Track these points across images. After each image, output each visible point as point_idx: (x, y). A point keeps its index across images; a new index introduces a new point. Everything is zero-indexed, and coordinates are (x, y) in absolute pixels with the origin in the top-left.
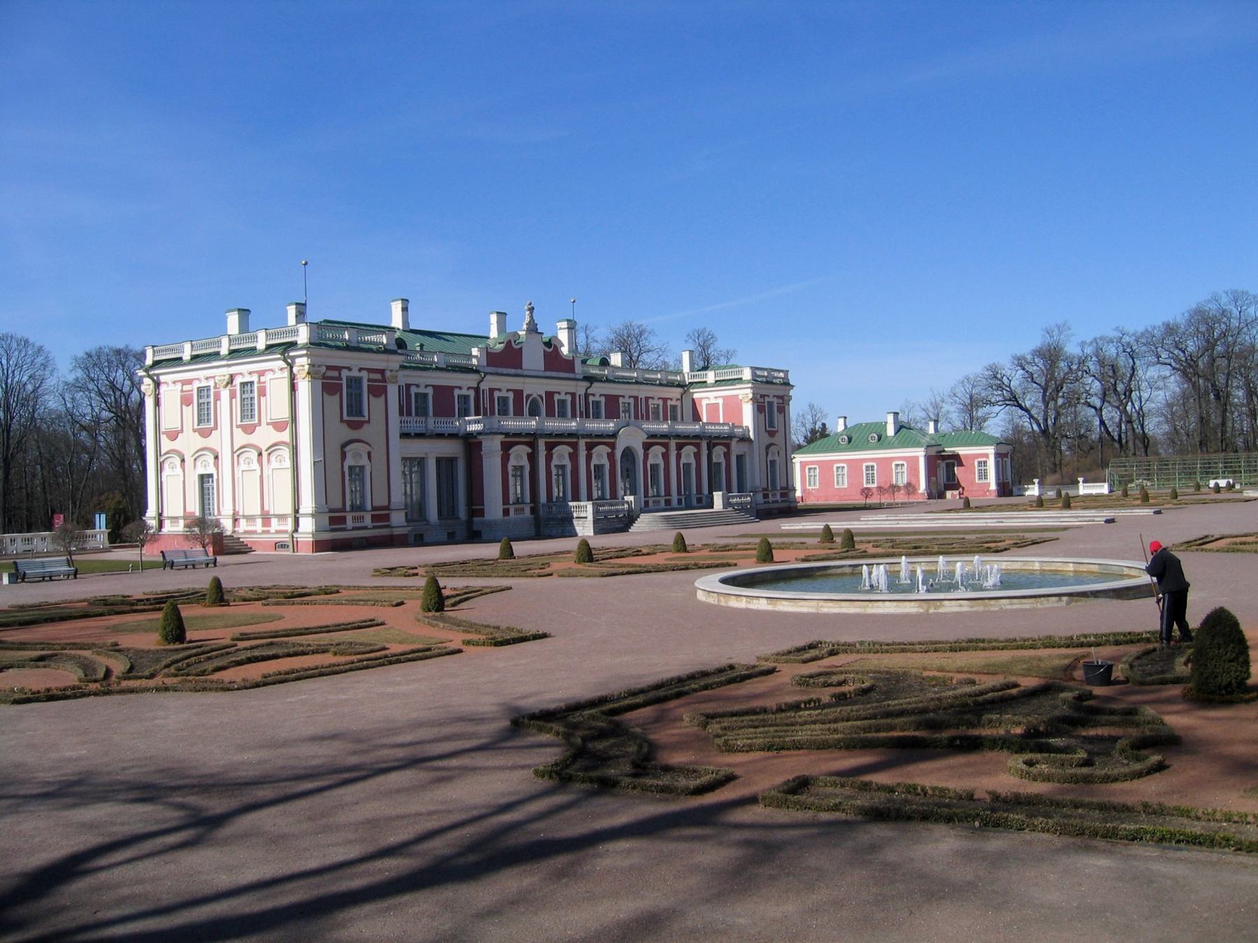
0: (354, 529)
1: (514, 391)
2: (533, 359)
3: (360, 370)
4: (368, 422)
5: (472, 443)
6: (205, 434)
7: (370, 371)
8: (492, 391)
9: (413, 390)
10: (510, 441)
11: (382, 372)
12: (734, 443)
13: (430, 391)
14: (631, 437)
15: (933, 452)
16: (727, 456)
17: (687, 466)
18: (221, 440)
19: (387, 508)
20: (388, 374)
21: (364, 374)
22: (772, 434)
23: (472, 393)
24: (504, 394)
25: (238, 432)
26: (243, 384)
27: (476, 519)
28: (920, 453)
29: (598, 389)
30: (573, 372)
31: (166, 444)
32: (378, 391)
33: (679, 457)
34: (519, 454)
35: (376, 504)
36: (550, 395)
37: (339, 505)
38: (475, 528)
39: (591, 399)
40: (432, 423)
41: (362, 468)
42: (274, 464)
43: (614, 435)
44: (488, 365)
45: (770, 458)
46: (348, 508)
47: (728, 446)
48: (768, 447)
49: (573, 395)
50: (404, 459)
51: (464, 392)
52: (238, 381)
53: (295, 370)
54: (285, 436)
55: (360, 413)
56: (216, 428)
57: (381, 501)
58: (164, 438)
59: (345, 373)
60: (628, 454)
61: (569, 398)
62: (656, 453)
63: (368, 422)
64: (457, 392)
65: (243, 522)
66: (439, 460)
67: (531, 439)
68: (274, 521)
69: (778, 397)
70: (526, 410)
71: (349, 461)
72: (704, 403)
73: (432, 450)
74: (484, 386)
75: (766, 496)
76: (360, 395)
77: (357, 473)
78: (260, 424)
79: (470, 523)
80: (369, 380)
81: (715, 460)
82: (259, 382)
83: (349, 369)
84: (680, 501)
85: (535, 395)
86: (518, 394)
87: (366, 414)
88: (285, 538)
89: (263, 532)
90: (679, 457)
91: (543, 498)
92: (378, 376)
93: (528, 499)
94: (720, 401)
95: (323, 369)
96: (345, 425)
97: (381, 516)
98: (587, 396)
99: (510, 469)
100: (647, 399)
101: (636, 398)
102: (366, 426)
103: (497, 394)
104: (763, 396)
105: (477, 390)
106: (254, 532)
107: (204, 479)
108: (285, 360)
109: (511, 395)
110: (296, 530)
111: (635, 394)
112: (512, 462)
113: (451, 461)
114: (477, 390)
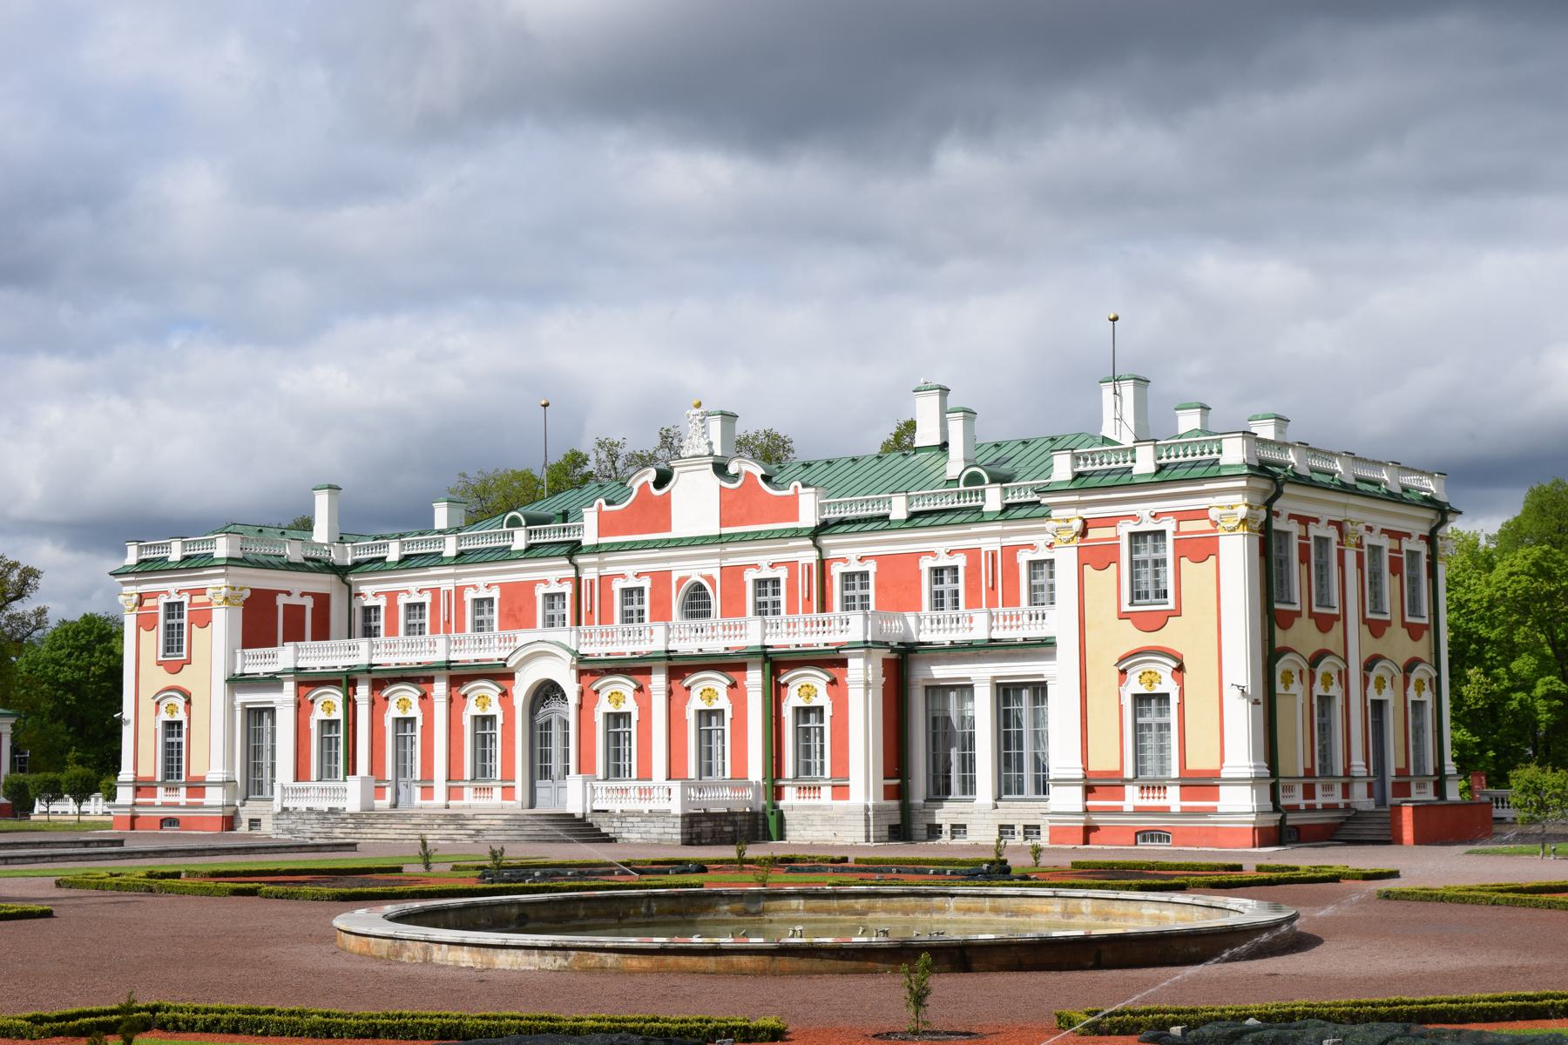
0: (164, 805)
1: (654, 575)
8: (605, 581)
9: (469, 595)
13: (495, 593)
14: (548, 655)
19: (202, 780)
23: (568, 589)
29: (848, 553)
36: (732, 575)
39: (836, 571)
41: (180, 724)
46: (159, 779)
48: (1122, 660)
49: (792, 565)
55: (180, 649)
60: (547, 691)
61: (782, 574)
62: (618, 694)
69: (1181, 516)
74: (589, 574)
77: (172, 727)
86: (662, 579)
97: (197, 787)
98: (823, 564)
99: (314, 726)
100: (1010, 552)
101: (973, 554)
105: (578, 581)
109: (646, 583)
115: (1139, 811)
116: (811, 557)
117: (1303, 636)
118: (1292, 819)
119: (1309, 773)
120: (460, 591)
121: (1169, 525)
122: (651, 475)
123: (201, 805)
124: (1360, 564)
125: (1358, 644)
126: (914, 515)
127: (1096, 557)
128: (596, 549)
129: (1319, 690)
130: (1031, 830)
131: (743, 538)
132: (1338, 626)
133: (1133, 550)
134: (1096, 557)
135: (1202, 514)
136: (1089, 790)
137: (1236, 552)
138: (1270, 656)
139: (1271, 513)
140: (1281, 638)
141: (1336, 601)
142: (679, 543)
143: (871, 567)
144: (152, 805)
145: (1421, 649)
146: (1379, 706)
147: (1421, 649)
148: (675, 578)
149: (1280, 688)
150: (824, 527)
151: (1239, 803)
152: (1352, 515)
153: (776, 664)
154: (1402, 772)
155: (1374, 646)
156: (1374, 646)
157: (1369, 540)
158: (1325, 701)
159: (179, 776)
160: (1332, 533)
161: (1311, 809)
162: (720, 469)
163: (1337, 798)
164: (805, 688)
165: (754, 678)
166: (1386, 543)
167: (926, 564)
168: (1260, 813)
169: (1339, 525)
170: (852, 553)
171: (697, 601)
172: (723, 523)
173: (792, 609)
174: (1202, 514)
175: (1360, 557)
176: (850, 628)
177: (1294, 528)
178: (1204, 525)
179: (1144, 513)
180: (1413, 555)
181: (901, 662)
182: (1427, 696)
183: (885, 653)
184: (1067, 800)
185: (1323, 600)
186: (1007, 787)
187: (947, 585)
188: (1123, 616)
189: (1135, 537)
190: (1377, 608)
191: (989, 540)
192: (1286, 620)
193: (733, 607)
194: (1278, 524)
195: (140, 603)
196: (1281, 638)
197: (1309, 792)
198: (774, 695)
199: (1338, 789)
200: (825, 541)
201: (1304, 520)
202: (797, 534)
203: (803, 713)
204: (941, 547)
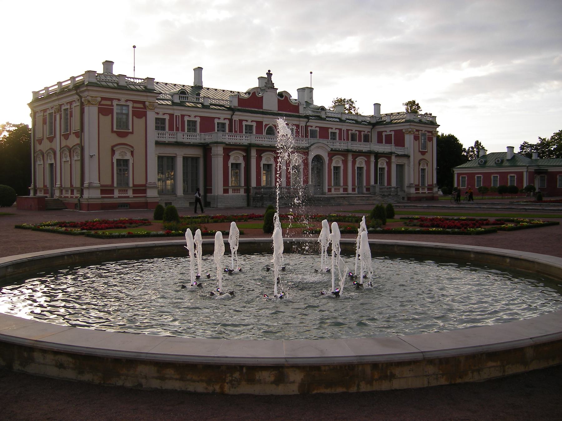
0: (119, 197)
1: (257, 122)
2: (270, 104)
3: (127, 101)
4: (132, 133)
5: (206, 148)
6: (51, 140)
7: (134, 102)
8: (241, 121)
9: (186, 119)
10: (228, 149)
11: (143, 103)
12: (393, 159)
13: (198, 120)
15: (532, 169)
16: (389, 164)
17: (360, 169)
18: (56, 145)
19: (145, 186)
20: (147, 104)
21: (130, 104)
22: (423, 153)
23: (227, 122)
24: (249, 123)
25: (62, 138)
26: (65, 110)
27: (208, 194)
28: (524, 170)
30: (298, 112)
31: (39, 147)
32: (140, 114)
33: (354, 163)
34: (237, 158)
35: (135, 183)
37: (109, 183)
38: (208, 200)
39: (309, 128)
40: (181, 137)
41: (127, 161)
42: (76, 158)
43: (308, 148)
44: (239, 106)
45: (421, 167)
47: (390, 158)
50: (160, 158)
51: (221, 121)
52: (63, 108)
53: (83, 99)
54: (77, 141)
56: (55, 137)
57: (140, 181)
58: (37, 143)
59: (115, 103)
60: (318, 158)
62: (337, 161)
63: (132, 133)
64: (216, 121)
65: (64, 191)
66: (185, 159)
67: (247, 149)
68: (75, 191)
69: (429, 132)
70: (264, 133)
71: (117, 156)
72: (384, 134)
73: (180, 154)
75: (417, 189)
76: (127, 115)
77: (123, 164)
78: (70, 134)
79: (205, 196)
80: (133, 107)
81: (379, 166)
82: (71, 108)
83: (119, 100)
84: (354, 190)
85: (271, 125)
86: (259, 124)
87: (130, 127)
88: (76, 201)
89: (72, 197)
90: (354, 163)
91: (254, 184)
92: (141, 106)
93: (243, 184)
94: (393, 133)
95: (99, 99)
96: (114, 135)
97: (140, 190)
98: (306, 127)
101: (340, 130)
102: (130, 136)
103: (244, 123)
104: (417, 131)
105: (231, 120)
106: (68, 197)
107: (51, 165)
108: (77, 94)
109: (254, 124)
110: (82, 197)
111: (340, 127)
112: (232, 161)
113: (195, 160)
114: (231, 120)
115: (422, 193)
120: (183, 116)
123: (145, 197)
127: (416, 138)
130: (403, 198)
144: (112, 197)
148: (264, 124)
153: (378, 156)
159: (127, 184)
164: (382, 163)
165: (373, 159)
172: (279, 109)
178: (430, 134)
195: (100, 102)
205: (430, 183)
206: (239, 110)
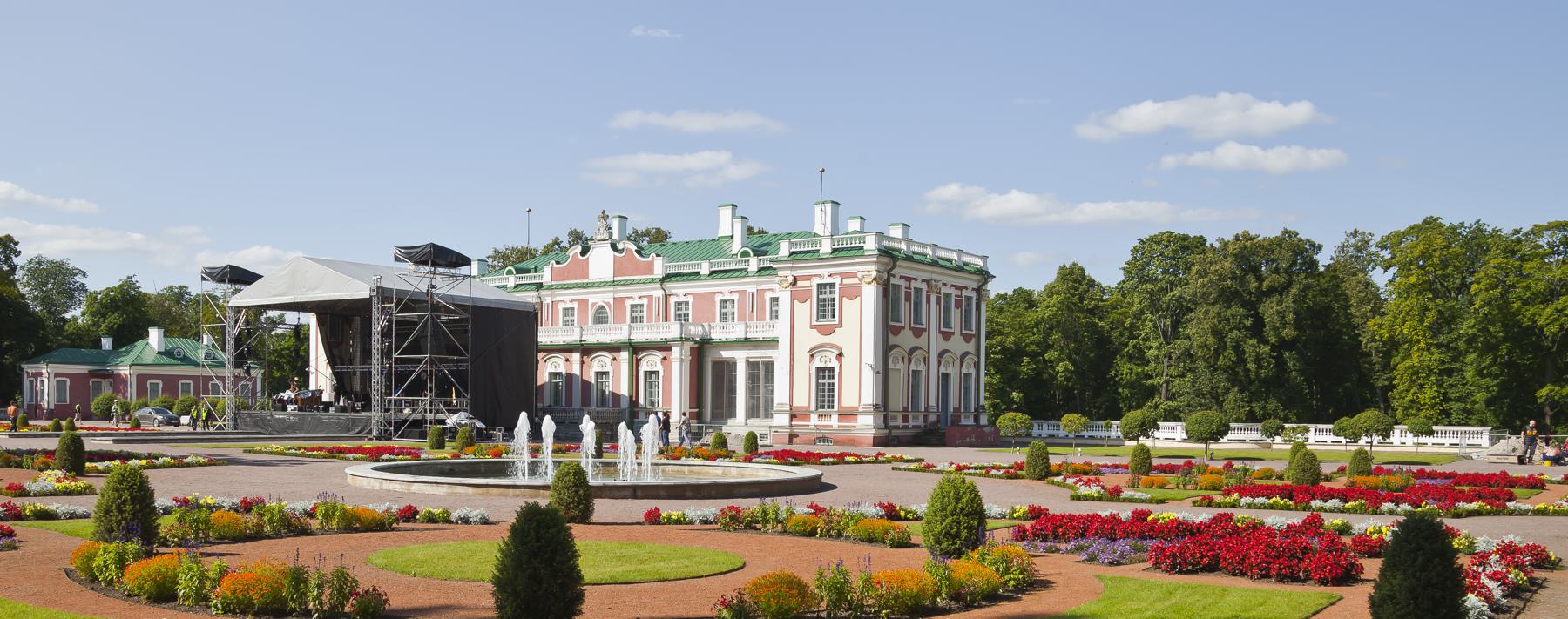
29: (680, 291)
36: (619, 302)
39: (672, 300)
49: (650, 297)
61: (645, 302)
69: (843, 276)
86: (583, 303)
98: (666, 297)
100: (761, 292)
101: (742, 293)
109: (575, 305)
116: (660, 293)
117: (906, 339)
118: (895, 433)
119: (906, 409)
121: (837, 280)
122: (579, 248)
124: (939, 302)
125: (936, 343)
126: (713, 273)
127: (798, 296)
128: (550, 287)
129: (913, 367)
131: (626, 283)
132: (925, 335)
133: (819, 293)
134: (798, 296)
135: (854, 275)
136: (793, 416)
137: (870, 294)
138: (886, 349)
139: (890, 275)
140: (893, 340)
141: (924, 320)
142: (593, 285)
143: (690, 299)
145: (971, 347)
146: (946, 376)
147: (971, 347)
149: (891, 366)
150: (667, 278)
151: (866, 424)
152: (935, 277)
153: (636, 349)
154: (957, 410)
155: (944, 345)
156: (944, 345)
157: (944, 290)
158: (916, 373)
160: (924, 286)
161: (906, 427)
162: (614, 247)
163: (920, 422)
164: (651, 361)
165: (624, 356)
166: (953, 292)
167: (718, 298)
168: (877, 428)
169: (928, 282)
170: (681, 292)
171: (601, 316)
173: (650, 320)
174: (854, 275)
175: (939, 299)
176: (673, 331)
177: (903, 283)
178: (855, 280)
179: (824, 274)
180: (968, 299)
181: (701, 349)
182: (972, 371)
183: (688, 345)
184: (782, 420)
185: (917, 320)
186: (752, 412)
187: (729, 309)
188: (812, 327)
189: (820, 286)
190: (947, 324)
191: (750, 286)
192: (897, 331)
193: (619, 319)
194: (893, 281)
196: (893, 340)
197: (905, 419)
198: (635, 365)
199: (921, 418)
200: (668, 285)
201: (909, 279)
202: (653, 281)
203: (650, 374)
204: (726, 289)
205: (849, 400)
206: (550, 287)
